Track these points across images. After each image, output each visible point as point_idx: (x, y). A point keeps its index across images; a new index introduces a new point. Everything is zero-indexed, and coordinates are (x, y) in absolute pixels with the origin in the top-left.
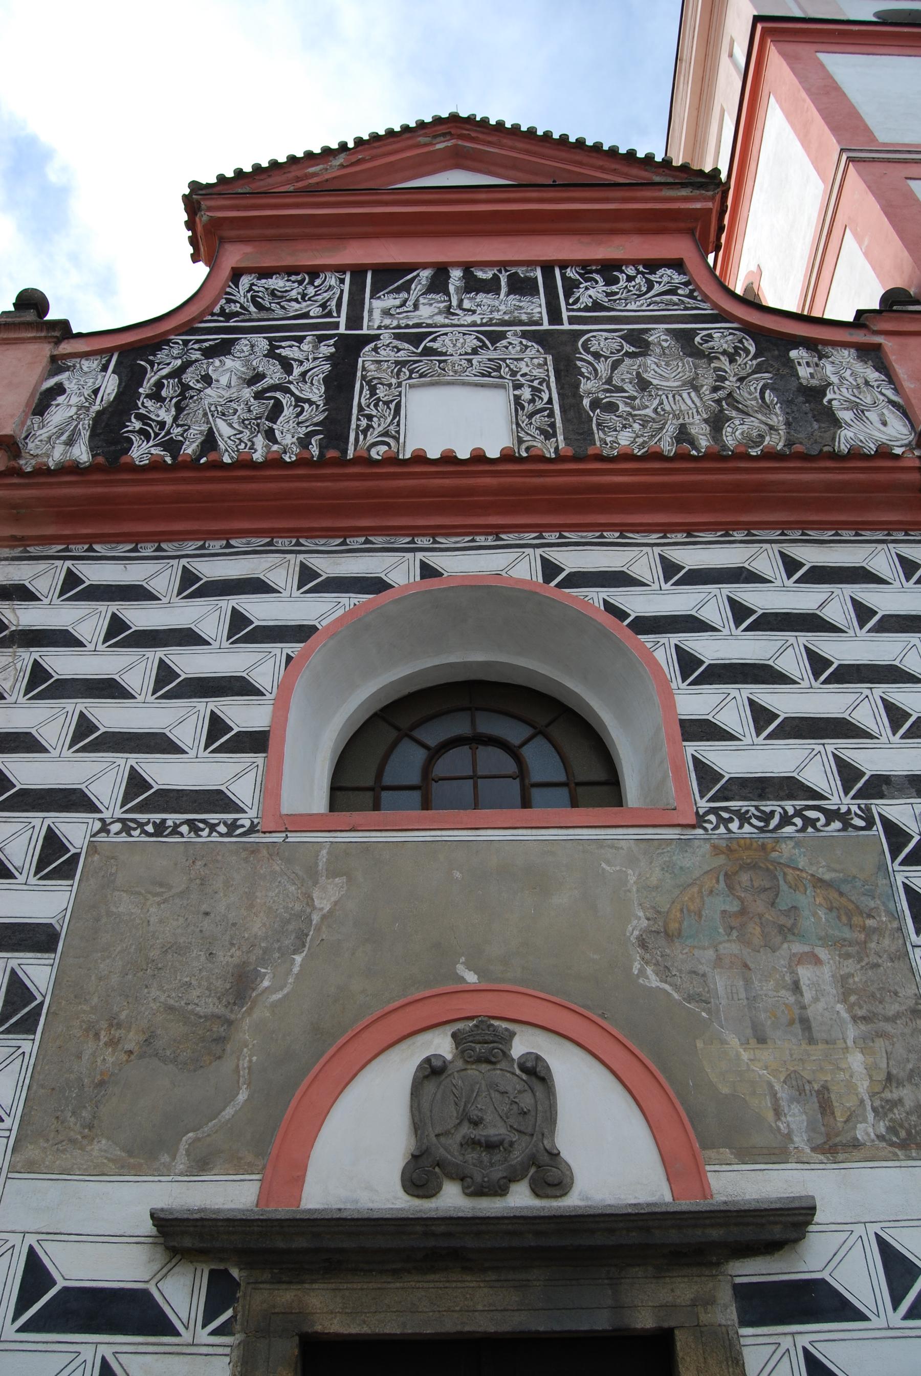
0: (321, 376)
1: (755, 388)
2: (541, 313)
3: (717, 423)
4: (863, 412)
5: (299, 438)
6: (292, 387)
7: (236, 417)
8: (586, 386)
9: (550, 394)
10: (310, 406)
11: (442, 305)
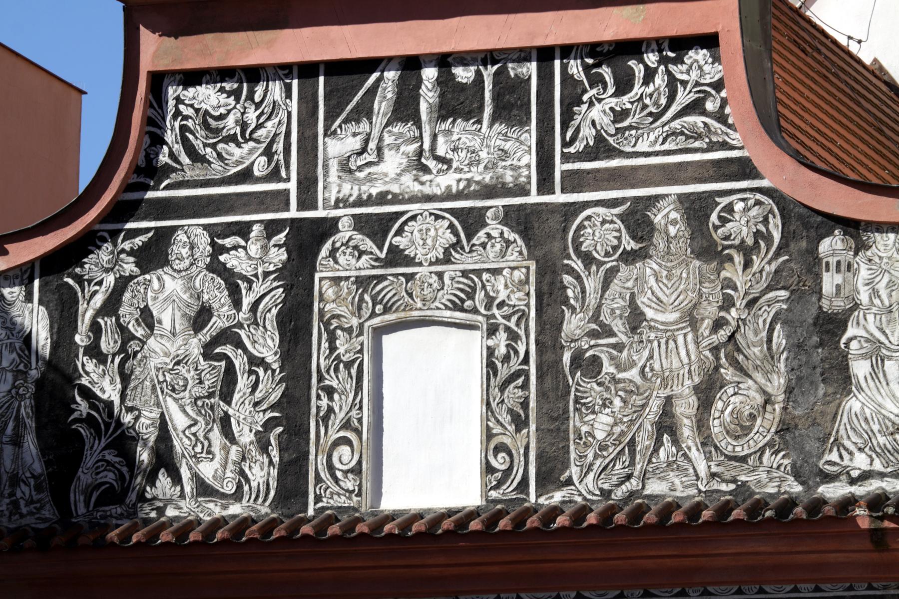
0: (274, 311)
1: (765, 321)
2: (528, 166)
3: (707, 391)
4: (883, 361)
5: (257, 433)
6: (242, 333)
7: (187, 392)
8: (574, 324)
9: (528, 344)
10: (266, 371)
11: (412, 148)
